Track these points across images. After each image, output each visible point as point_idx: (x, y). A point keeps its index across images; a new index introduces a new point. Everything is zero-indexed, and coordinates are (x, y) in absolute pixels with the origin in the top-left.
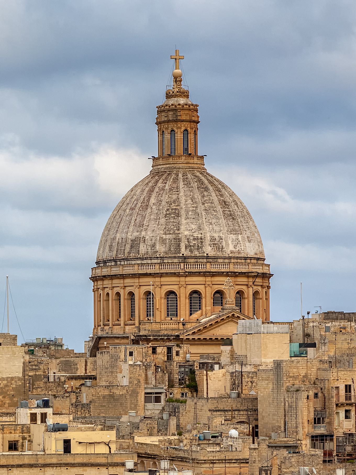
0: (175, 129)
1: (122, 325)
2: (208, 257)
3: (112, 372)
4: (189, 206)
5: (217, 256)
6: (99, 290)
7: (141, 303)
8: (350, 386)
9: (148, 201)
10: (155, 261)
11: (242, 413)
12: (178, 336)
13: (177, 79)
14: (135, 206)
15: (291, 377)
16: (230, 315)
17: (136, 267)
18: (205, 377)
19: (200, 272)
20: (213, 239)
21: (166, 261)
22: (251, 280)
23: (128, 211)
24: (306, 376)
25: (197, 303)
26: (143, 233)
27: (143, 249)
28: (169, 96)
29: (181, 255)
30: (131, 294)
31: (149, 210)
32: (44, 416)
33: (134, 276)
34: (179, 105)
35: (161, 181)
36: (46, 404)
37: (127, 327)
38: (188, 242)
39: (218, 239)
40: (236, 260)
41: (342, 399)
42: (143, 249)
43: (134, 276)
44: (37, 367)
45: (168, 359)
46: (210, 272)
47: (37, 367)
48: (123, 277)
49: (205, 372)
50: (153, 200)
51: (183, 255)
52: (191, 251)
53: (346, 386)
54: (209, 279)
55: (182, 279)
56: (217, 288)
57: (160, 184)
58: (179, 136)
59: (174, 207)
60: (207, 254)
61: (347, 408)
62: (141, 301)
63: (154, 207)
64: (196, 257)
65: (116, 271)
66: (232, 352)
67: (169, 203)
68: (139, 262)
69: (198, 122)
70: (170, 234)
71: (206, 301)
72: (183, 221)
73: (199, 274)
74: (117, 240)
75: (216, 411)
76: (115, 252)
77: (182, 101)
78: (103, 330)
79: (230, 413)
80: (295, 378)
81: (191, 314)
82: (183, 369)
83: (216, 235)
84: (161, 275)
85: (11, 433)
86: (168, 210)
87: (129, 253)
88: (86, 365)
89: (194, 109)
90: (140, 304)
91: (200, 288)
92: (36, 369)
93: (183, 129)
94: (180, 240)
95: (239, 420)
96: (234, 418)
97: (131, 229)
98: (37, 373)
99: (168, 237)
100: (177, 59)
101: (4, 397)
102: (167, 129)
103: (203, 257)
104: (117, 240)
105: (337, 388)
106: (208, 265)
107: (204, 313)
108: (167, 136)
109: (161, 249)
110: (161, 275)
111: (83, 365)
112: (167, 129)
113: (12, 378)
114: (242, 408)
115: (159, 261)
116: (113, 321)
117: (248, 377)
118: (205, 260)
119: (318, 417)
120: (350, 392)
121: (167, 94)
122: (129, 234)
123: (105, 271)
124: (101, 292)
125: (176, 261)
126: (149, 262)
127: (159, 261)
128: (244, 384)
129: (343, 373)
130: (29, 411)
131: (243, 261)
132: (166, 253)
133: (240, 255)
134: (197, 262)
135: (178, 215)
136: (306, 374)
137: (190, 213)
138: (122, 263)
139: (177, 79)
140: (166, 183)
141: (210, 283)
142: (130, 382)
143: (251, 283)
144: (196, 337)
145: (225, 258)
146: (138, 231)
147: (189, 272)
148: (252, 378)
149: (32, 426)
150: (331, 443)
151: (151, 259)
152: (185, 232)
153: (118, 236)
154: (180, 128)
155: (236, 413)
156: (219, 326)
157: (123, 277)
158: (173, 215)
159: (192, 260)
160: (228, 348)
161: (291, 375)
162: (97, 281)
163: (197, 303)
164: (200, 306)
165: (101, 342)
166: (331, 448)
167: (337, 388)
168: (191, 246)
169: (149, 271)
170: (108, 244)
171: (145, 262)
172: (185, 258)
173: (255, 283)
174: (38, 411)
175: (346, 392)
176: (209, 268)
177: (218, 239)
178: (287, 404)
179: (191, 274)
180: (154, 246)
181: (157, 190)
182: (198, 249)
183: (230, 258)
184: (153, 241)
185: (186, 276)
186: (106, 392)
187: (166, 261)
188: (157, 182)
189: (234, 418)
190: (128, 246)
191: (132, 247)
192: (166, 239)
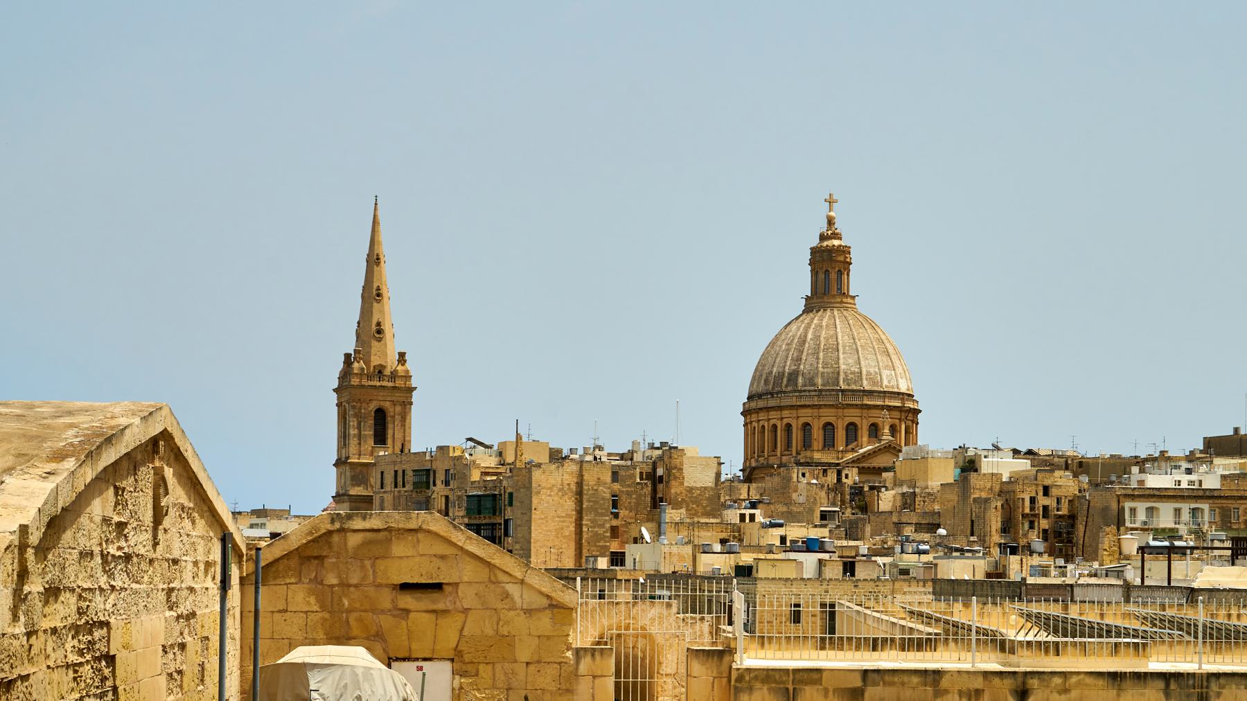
0: (829, 269)
1: (779, 455)
2: (864, 391)
3: (783, 493)
4: (846, 341)
6: (754, 423)
7: (799, 434)
8: (1034, 497)
9: (806, 336)
10: (814, 393)
13: (830, 222)
14: (792, 341)
15: (977, 489)
17: (794, 399)
18: (876, 498)
20: (869, 373)
21: (823, 393)
22: (903, 414)
23: (784, 346)
24: (991, 489)
28: (823, 237)
29: (839, 388)
30: (789, 426)
31: (807, 345)
32: (752, 517)
33: (792, 407)
35: (816, 318)
36: (753, 505)
37: (784, 458)
38: (846, 376)
40: (890, 395)
41: (1027, 511)
42: (800, 380)
43: (792, 407)
45: (837, 481)
48: (780, 408)
49: (876, 493)
50: (810, 336)
53: (1031, 497)
56: (872, 420)
57: (815, 321)
58: (833, 276)
61: (1031, 519)
62: (799, 431)
63: (811, 342)
65: (772, 403)
66: (895, 477)
67: (827, 339)
68: (797, 394)
69: (851, 263)
71: (862, 433)
72: (841, 356)
74: (774, 374)
76: (771, 387)
77: (836, 242)
78: (757, 461)
80: (981, 490)
83: (872, 370)
84: (819, 407)
85: (722, 531)
86: (825, 345)
87: (786, 386)
88: (749, 491)
89: (845, 251)
90: (796, 435)
91: (857, 420)
93: (837, 269)
97: (788, 363)
99: (826, 370)
100: (831, 202)
101: (698, 506)
102: (821, 268)
103: (860, 391)
104: (774, 374)
105: (1023, 499)
108: (822, 276)
110: (819, 407)
111: (746, 490)
112: (821, 268)
113: (705, 488)
115: (817, 393)
116: (768, 452)
117: (921, 497)
118: (862, 393)
120: (1034, 503)
121: (820, 236)
122: (787, 368)
123: (761, 404)
124: (755, 424)
125: (834, 393)
127: (817, 393)
128: (917, 503)
130: (739, 512)
131: (896, 396)
134: (854, 395)
137: (847, 348)
138: (779, 395)
139: (830, 222)
140: (822, 320)
141: (866, 415)
142: (807, 500)
143: (903, 417)
146: (795, 365)
147: (847, 404)
148: (924, 497)
149: (743, 524)
153: (775, 370)
154: (834, 268)
156: (876, 456)
157: (780, 408)
159: (850, 393)
160: (892, 474)
161: (978, 487)
162: (751, 414)
164: (856, 437)
165: (755, 472)
167: (1023, 499)
169: (807, 403)
170: (764, 377)
171: (803, 394)
172: (843, 391)
173: (908, 418)
174: (748, 512)
175: (1031, 503)
178: (974, 514)
181: (813, 326)
182: (855, 383)
184: (812, 374)
186: (785, 509)
188: (812, 319)
190: (785, 379)
191: (789, 380)
192: (823, 373)
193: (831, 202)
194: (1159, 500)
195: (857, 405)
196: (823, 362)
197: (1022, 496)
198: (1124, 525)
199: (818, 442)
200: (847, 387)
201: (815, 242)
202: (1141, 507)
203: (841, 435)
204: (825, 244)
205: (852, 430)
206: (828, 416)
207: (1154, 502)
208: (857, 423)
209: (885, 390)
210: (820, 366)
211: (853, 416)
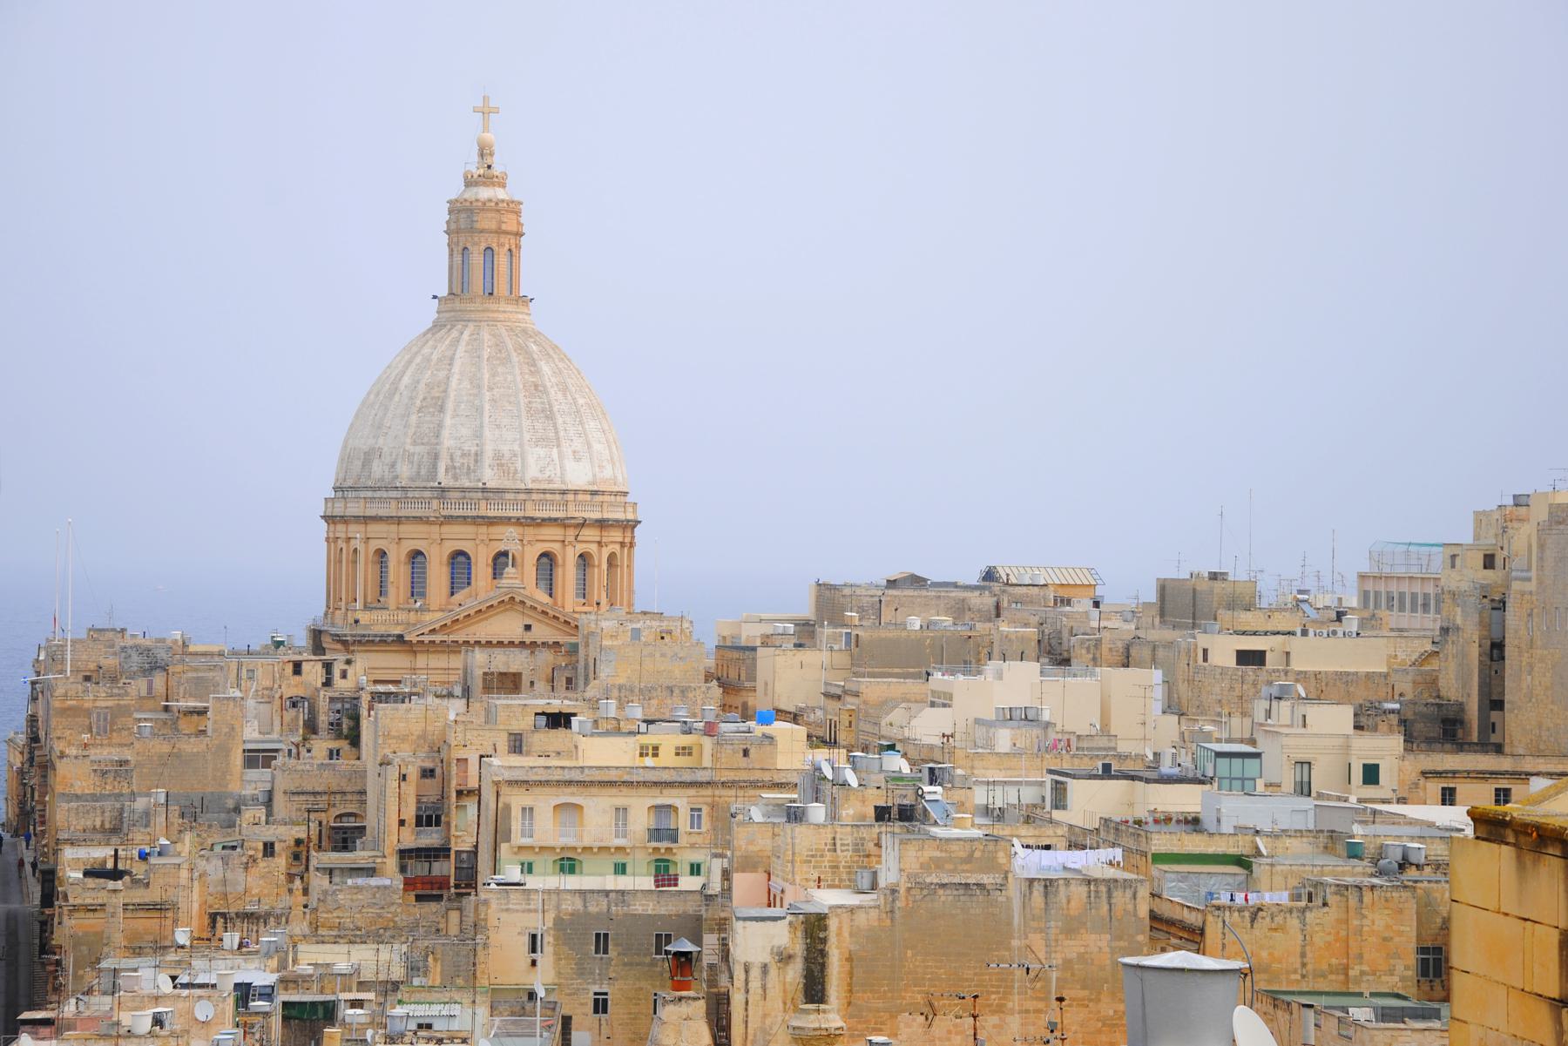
2: (484, 490)
5: (502, 487)
7: (370, 570)
11: (349, 797)
12: (401, 636)
13: (484, 151)
16: (506, 598)
19: (465, 517)
20: (498, 456)
21: (410, 494)
22: (571, 532)
25: (463, 573)
26: (381, 441)
27: (378, 469)
28: (470, 183)
29: (436, 484)
34: (477, 200)
38: (452, 459)
39: (507, 455)
40: (542, 495)
44: (122, 691)
46: (483, 517)
47: (122, 691)
50: (406, 380)
51: (440, 483)
52: (456, 478)
54: (483, 529)
55: (435, 528)
59: (437, 395)
60: (484, 484)
64: (463, 490)
68: (369, 494)
70: (423, 444)
72: (448, 421)
73: (464, 520)
75: (298, 793)
79: (325, 798)
81: (452, 594)
82: (339, 706)
83: (505, 449)
84: (399, 520)
86: (424, 399)
89: (514, 208)
92: (119, 695)
93: (483, 246)
94: (436, 457)
95: (343, 811)
96: (334, 805)
98: (122, 702)
99: (419, 449)
100: (486, 111)
103: (475, 490)
106: (483, 503)
107: (474, 593)
109: (405, 472)
110: (399, 520)
114: (349, 789)
119: (428, 813)
125: (427, 494)
126: (384, 494)
129: (475, 733)
131: (558, 497)
132: (412, 479)
133: (551, 486)
134: (464, 498)
135: (442, 409)
136: (425, 731)
137: (463, 406)
139: (484, 151)
141: (485, 537)
143: (572, 539)
144: (438, 638)
145: (518, 491)
147: (445, 517)
150: (445, 864)
151: (387, 489)
152: (447, 442)
155: (338, 797)
158: (431, 410)
161: (393, 733)
163: (463, 573)
166: (445, 873)
168: (455, 468)
171: (378, 494)
173: (579, 538)
176: (484, 510)
177: (507, 455)
179: (450, 520)
180: (393, 465)
182: (468, 474)
183: (529, 491)
184: (394, 457)
185: (441, 524)
187: (410, 494)
189: (334, 805)
192: (413, 454)
193: (486, 111)
194: (581, 790)
195: (465, 518)
196: (414, 434)
197: (462, 754)
198: (508, 840)
199: (398, 588)
200: (452, 484)
201: (456, 189)
202: (544, 803)
203: (438, 574)
204: (471, 194)
205: (460, 562)
206: (415, 537)
207: (573, 794)
208: (469, 553)
209: (530, 486)
210: (409, 441)
211: (460, 537)
